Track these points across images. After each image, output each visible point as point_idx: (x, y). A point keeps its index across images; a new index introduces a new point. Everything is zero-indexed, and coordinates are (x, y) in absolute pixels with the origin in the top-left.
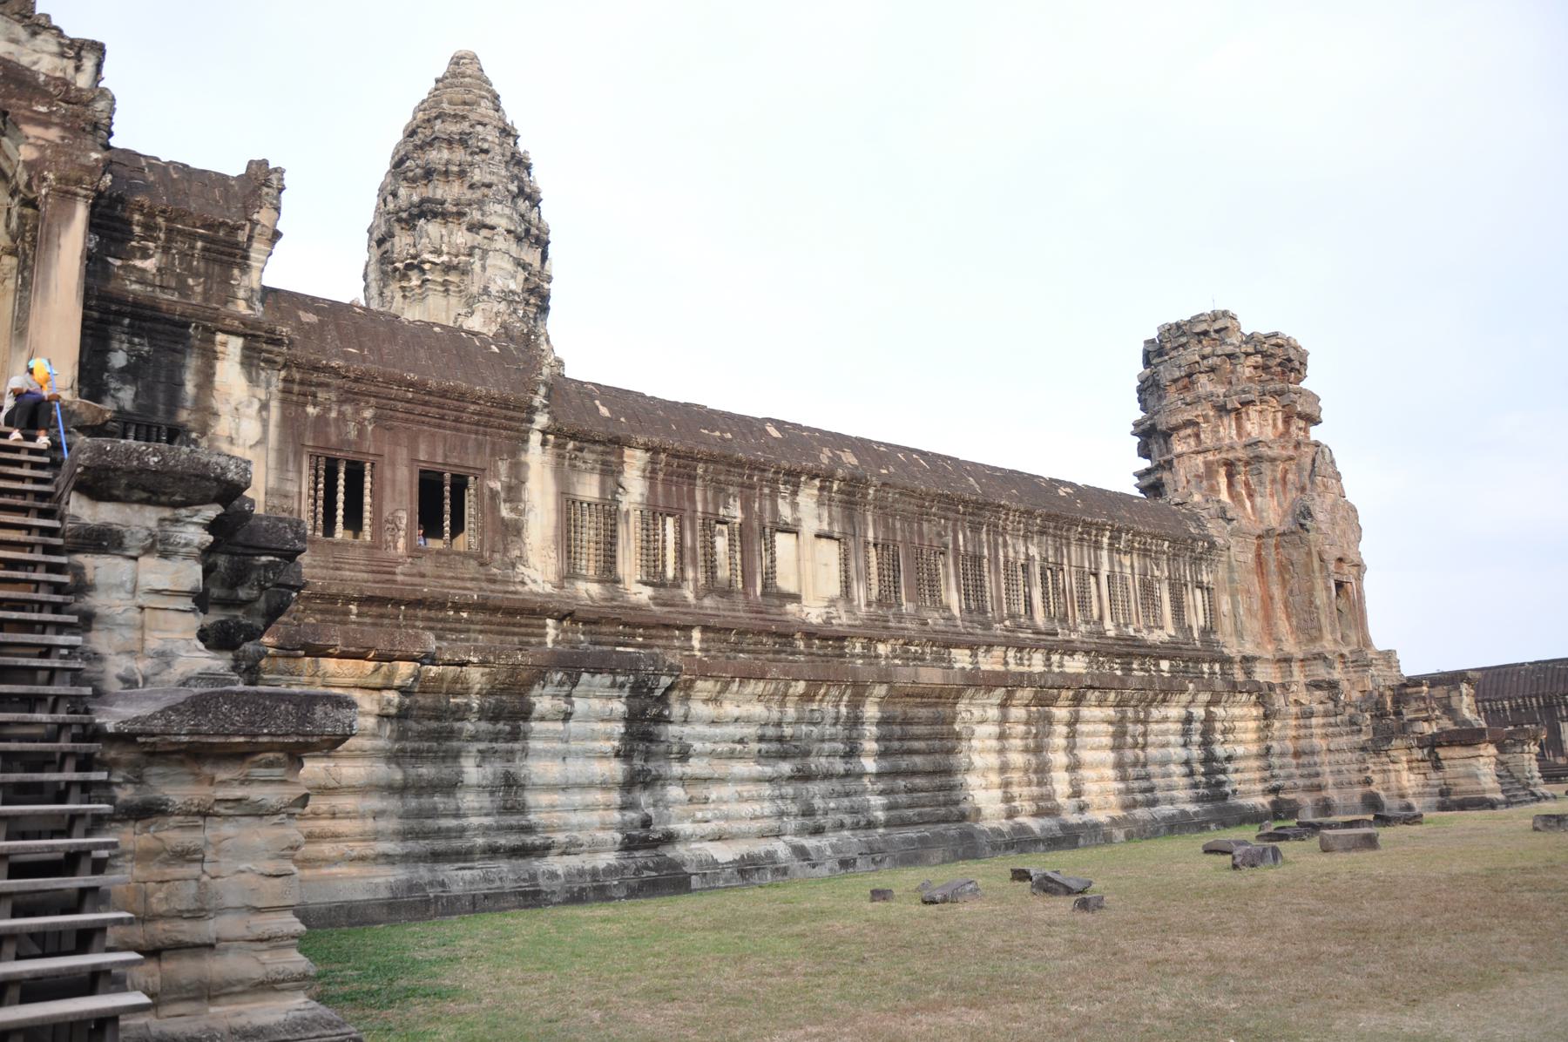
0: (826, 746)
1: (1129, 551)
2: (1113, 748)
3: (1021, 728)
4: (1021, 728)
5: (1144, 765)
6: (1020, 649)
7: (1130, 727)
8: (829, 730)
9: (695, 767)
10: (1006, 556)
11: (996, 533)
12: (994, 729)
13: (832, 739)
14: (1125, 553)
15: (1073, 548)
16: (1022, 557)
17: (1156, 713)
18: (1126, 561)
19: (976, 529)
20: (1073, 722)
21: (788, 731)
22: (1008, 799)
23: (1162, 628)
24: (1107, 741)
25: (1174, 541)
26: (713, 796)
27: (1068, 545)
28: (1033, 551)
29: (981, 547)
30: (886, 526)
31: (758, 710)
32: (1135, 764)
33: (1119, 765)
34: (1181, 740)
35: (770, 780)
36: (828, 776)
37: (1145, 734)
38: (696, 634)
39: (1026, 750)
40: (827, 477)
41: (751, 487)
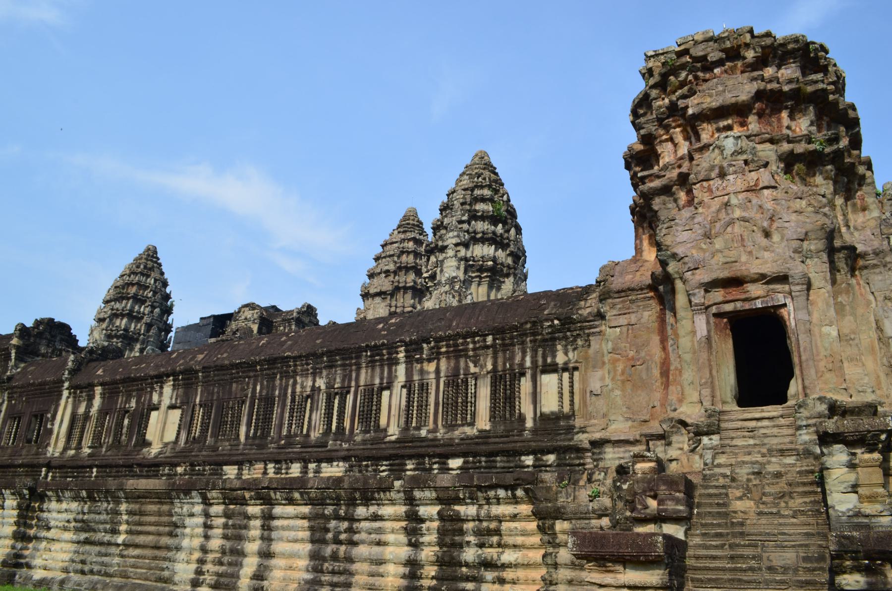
0: (101, 527)
1: (435, 356)
2: (312, 541)
3: (221, 521)
4: (221, 521)
5: (350, 560)
6: (277, 462)
7: (333, 524)
8: (103, 517)
9: (51, 534)
10: (294, 392)
11: (288, 377)
12: (200, 520)
13: (105, 522)
14: (430, 360)
15: (363, 371)
16: (309, 389)
17: (361, 511)
18: (431, 367)
19: (272, 378)
20: (268, 517)
21: (86, 517)
22: (199, 572)
23: (472, 424)
24: (307, 534)
25: (498, 332)
26: (53, 549)
27: (359, 369)
28: (321, 383)
29: (274, 389)
30: (208, 394)
31: (74, 505)
32: (335, 557)
33: (315, 556)
34: (403, 538)
35: (73, 542)
36: (101, 544)
37: (350, 530)
38: (95, 470)
39: (225, 537)
40: (174, 374)
41: (142, 389)
